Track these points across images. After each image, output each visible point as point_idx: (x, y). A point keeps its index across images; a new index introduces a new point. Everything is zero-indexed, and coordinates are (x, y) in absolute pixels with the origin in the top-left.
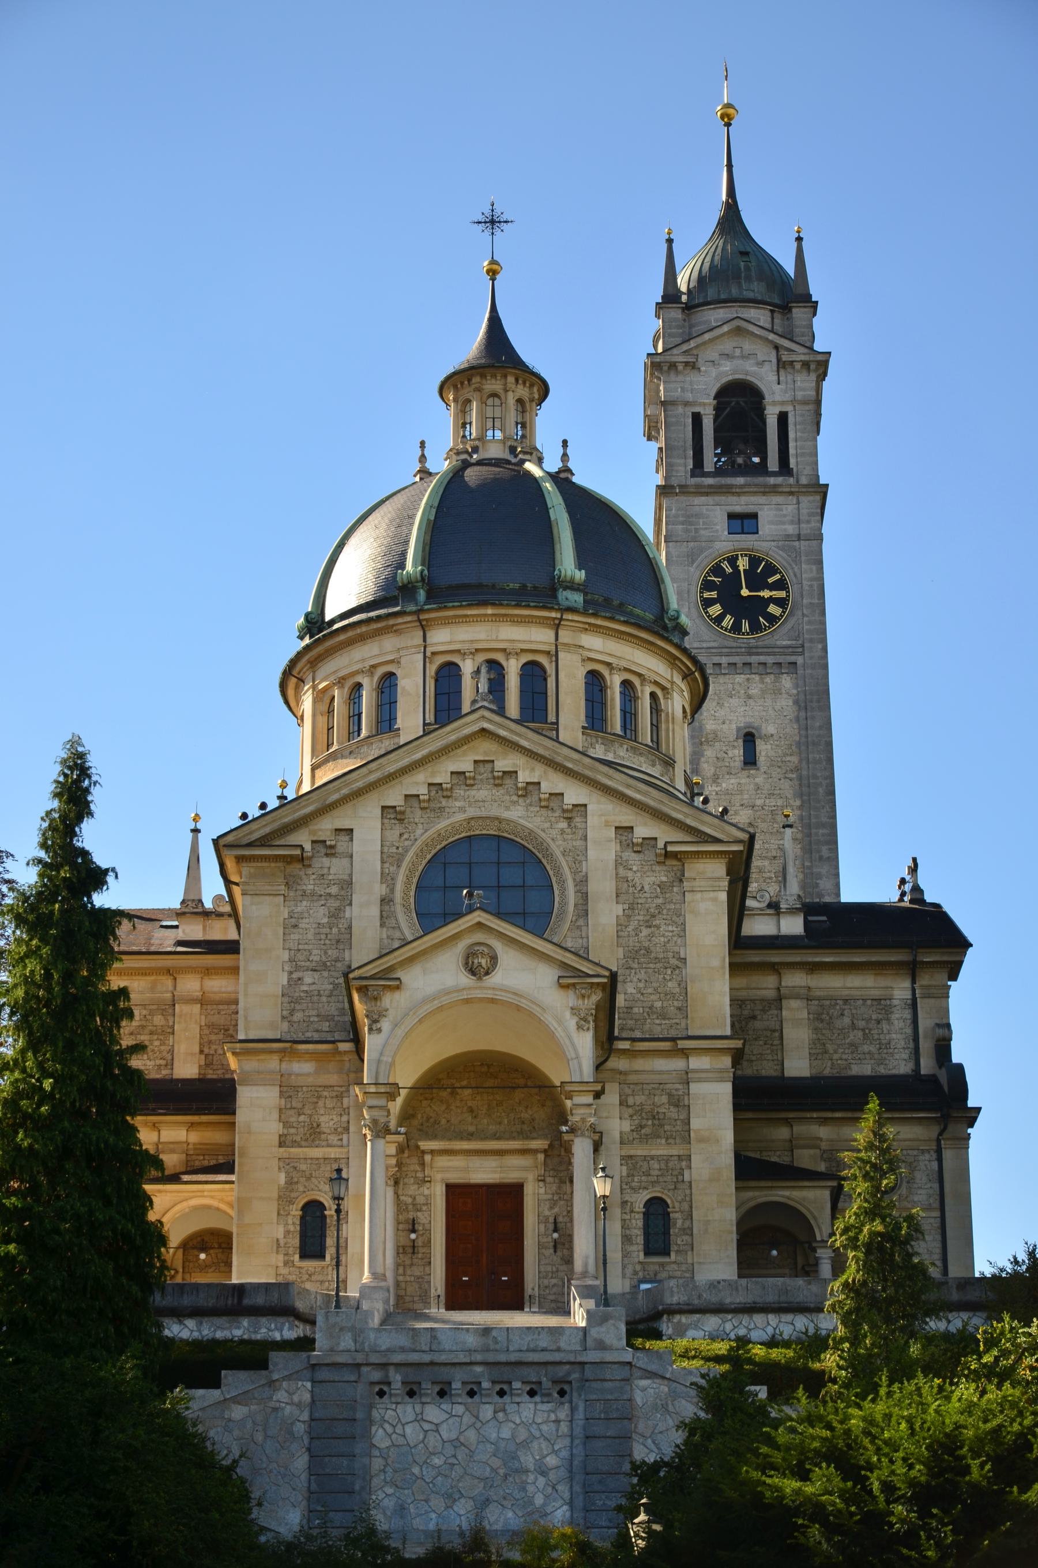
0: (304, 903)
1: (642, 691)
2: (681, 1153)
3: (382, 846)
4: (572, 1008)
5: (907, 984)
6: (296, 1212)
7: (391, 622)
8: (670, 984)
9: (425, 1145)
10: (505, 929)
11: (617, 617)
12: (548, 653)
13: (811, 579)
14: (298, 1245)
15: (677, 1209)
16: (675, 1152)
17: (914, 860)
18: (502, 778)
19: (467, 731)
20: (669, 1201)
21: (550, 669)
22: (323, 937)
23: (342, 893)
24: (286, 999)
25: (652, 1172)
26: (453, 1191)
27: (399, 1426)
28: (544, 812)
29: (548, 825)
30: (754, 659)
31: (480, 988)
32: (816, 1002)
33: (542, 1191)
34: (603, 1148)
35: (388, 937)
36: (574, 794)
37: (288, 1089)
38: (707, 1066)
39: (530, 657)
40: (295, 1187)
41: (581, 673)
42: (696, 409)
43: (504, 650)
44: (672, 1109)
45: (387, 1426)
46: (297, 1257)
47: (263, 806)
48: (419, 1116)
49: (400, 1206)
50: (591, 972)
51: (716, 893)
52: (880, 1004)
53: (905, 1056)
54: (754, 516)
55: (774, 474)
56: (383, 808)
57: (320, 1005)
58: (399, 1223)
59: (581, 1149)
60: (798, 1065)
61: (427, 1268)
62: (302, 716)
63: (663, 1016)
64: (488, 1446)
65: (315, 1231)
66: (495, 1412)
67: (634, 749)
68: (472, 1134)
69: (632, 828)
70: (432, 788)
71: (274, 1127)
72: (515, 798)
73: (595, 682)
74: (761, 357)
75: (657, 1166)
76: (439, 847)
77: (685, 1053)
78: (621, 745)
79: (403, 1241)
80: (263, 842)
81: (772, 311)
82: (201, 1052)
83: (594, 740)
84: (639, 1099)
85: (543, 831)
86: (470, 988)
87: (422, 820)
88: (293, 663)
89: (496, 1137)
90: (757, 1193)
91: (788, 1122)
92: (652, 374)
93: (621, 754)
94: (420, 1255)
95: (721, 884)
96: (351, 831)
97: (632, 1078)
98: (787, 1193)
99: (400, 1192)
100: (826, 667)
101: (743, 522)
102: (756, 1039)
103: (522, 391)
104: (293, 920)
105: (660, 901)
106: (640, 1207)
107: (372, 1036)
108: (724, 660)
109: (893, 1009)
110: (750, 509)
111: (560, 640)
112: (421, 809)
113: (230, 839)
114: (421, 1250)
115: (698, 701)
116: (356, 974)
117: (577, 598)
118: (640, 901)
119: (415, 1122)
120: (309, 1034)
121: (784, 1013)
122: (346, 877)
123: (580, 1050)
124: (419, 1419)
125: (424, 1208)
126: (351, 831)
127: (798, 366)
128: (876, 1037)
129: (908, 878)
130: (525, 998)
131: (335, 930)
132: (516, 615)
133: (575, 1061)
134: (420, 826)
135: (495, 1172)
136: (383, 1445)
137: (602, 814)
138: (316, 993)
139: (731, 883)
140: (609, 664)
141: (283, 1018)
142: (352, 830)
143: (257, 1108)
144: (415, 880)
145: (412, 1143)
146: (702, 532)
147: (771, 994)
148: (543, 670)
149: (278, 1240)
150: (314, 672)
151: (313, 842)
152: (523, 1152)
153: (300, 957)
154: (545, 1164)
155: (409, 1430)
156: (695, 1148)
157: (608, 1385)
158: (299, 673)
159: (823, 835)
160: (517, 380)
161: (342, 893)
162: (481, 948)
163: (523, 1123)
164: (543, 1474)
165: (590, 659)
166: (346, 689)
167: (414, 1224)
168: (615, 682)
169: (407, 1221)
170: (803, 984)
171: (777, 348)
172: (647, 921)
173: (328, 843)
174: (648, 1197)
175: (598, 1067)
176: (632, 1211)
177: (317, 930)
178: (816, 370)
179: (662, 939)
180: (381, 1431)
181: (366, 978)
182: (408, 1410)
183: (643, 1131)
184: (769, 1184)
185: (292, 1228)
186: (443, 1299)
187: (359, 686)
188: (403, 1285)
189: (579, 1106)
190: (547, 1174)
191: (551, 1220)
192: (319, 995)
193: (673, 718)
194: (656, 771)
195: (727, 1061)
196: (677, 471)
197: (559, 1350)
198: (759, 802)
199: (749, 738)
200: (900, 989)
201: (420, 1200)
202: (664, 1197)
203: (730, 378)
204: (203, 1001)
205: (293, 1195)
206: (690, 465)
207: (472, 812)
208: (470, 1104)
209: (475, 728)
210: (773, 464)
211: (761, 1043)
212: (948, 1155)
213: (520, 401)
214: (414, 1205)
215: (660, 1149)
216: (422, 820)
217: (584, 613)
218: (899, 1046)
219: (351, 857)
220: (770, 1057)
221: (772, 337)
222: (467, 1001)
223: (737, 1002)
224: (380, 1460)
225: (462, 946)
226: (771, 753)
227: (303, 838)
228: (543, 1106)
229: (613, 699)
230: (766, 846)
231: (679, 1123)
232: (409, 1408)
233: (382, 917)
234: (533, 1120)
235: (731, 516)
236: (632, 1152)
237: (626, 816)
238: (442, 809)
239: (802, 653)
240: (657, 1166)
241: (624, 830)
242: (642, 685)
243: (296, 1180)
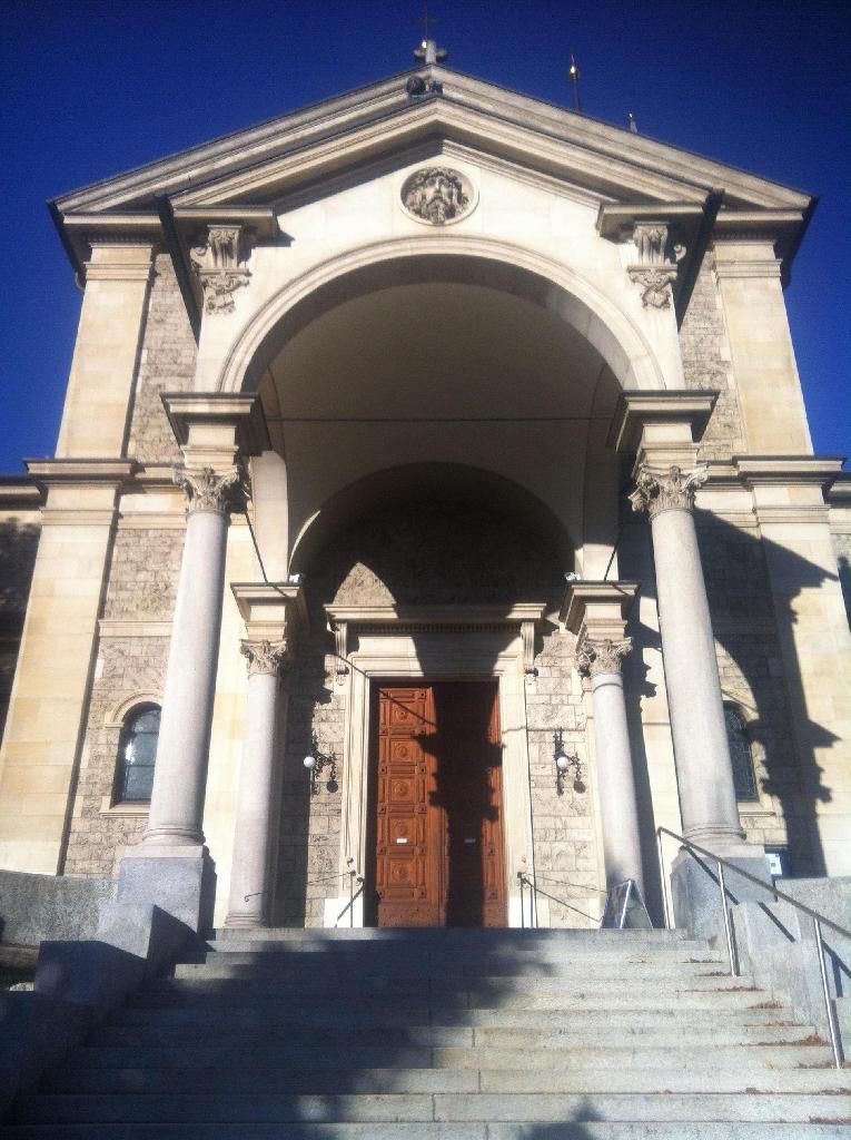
4: (630, 270)
10: (488, 130)
31: (439, 236)
38: (786, 501)
40: (117, 682)
46: (107, 800)
51: (763, 279)
86: (418, 238)
95: (771, 268)
123: (653, 343)
130: (532, 252)
133: (647, 362)
153: (164, 359)
179: (692, 338)
185: (104, 750)
225: (400, 176)
243: (120, 671)
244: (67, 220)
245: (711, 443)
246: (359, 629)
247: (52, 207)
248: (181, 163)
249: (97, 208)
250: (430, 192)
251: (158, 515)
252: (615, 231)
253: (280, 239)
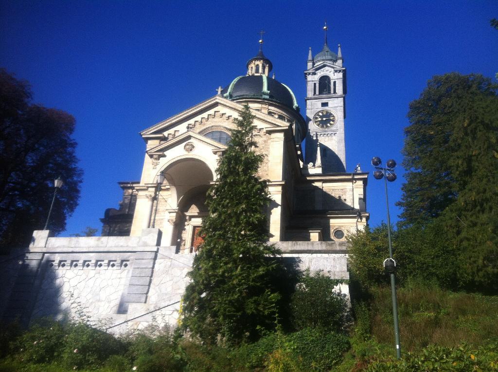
30: (326, 133)
72: (225, 120)
101: (325, 104)
110: (327, 102)
157: (144, 261)
164: (109, 302)
171: (333, 68)
197: (127, 246)
206: (313, 93)
210: (332, 91)
227: (166, 134)
238: (205, 124)
244: (143, 136)
246: (191, 217)
247: (140, 134)
248: (165, 122)
249: (148, 133)
250: (188, 147)
252: (215, 153)
253: (164, 156)
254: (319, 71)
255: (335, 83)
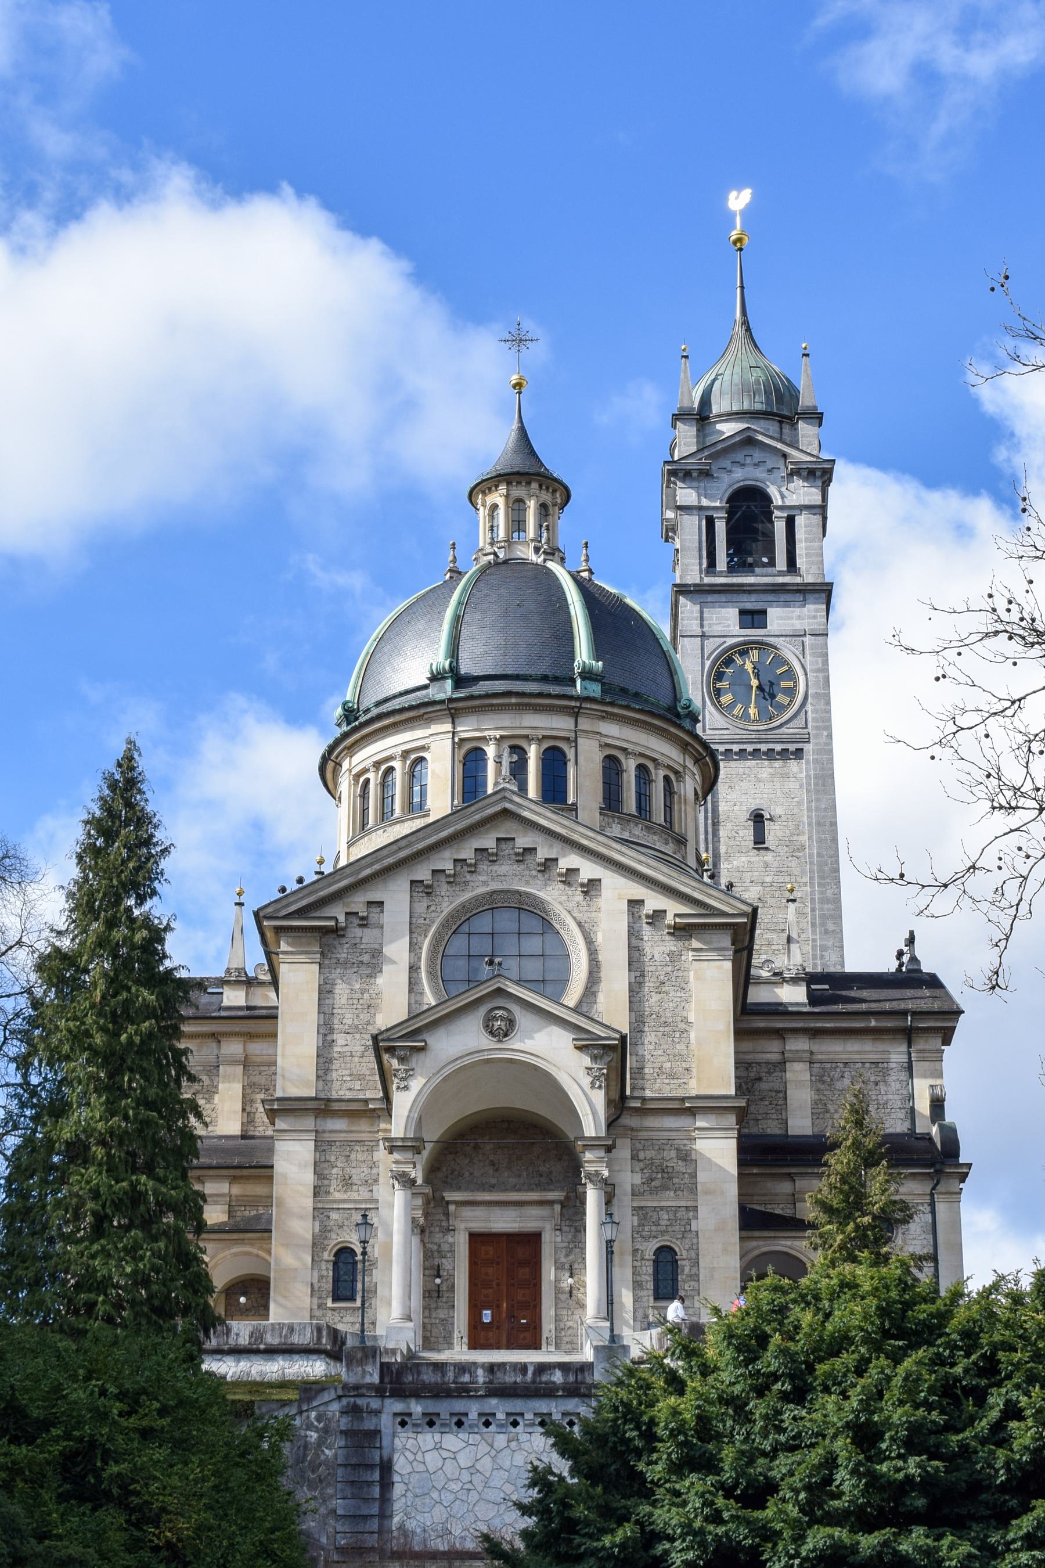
0: (338, 970)
1: (656, 774)
2: (689, 1204)
3: (411, 917)
5: (904, 1048)
6: (328, 1256)
7: (422, 711)
8: (678, 1046)
9: (450, 1196)
11: (633, 705)
12: (567, 739)
13: (818, 671)
14: (331, 1289)
15: (684, 1257)
16: (683, 1204)
17: (912, 933)
18: (523, 854)
19: (490, 811)
20: (677, 1249)
21: (570, 754)
22: (355, 1002)
23: (374, 961)
24: (321, 1060)
25: (662, 1223)
26: (477, 1239)
27: (420, 1453)
28: (561, 886)
29: (564, 898)
32: (818, 1065)
33: (559, 1239)
34: (615, 1201)
35: (416, 1002)
36: (589, 870)
37: (322, 1145)
39: (552, 743)
40: (328, 1234)
41: (598, 757)
42: (709, 513)
43: (526, 737)
44: (680, 1163)
45: (407, 1453)
47: (300, 880)
48: (444, 1169)
49: (428, 1255)
50: (603, 1035)
52: (877, 1067)
53: (902, 1116)
54: (764, 612)
55: (781, 574)
56: (412, 882)
57: (353, 1065)
58: (425, 1269)
59: (592, 1197)
60: (800, 1124)
61: (451, 1312)
62: (340, 798)
63: (672, 1076)
64: (502, 1472)
65: (347, 1274)
66: (509, 1441)
67: (648, 828)
68: (493, 1186)
69: (643, 901)
70: (457, 864)
71: (309, 1177)
72: (534, 873)
73: (612, 767)
74: (770, 465)
75: (666, 1217)
76: (463, 919)
77: (692, 1112)
78: (637, 825)
79: (430, 1286)
80: (300, 913)
81: (781, 422)
82: (244, 1110)
83: (611, 820)
84: (650, 1154)
85: (560, 903)
87: (448, 894)
88: (331, 749)
89: (515, 1188)
90: (761, 1243)
91: (791, 1177)
92: (669, 481)
93: (637, 832)
94: (444, 1300)
96: (381, 904)
97: (644, 1135)
98: (789, 1243)
99: (426, 1240)
100: (830, 752)
102: (761, 1100)
103: (546, 497)
104: (328, 986)
105: (669, 969)
106: (649, 1254)
107: (399, 1093)
108: (736, 748)
109: (891, 1072)
111: (579, 727)
112: (449, 883)
113: (269, 910)
114: (446, 1295)
115: (709, 784)
116: (384, 1036)
117: (595, 689)
118: (650, 969)
119: (440, 1175)
120: (341, 1093)
121: (788, 1075)
122: (377, 946)
124: (438, 1447)
125: (449, 1255)
126: (381, 904)
127: (804, 473)
128: (874, 1097)
129: (905, 949)
131: (366, 996)
132: (539, 705)
134: (446, 899)
135: (515, 1221)
136: (404, 1472)
137: (616, 889)
138: (349, 1054)
139: (736, 952)
140: (624, 750)
141: (318, 1077)
142: (382, 903)
143: (294, 1160)
144: (441, 949)
145: (437, 1195)
146: (715, 628)
147: (775, 1057)
148: (564, 755)
149: (312, 1284)
150: (351, 757)
151: (346, 914)
152: (541, 1203)
154: (562, 1214)
155: (429, 1457)
156: (701, 1199)
158: (337, 758)
159: (829, 910)
160: (540, 486)
161: (374, 961)
162: (500, 1013)
163: (541, 1176)
165: (607, 745)
166: (380, 773)
167: (439, 1271)
168: (630, 765)
169: (432, 1268)
170: (807, 1048)
172: (658, 987)
173: (360, 914)
174: (658, 1245)
175: (610, 1125)
176: (642, 1259)
177: (350, 996)
178: (822, 476)
179: (671, 1004)
180: (402, 1458)
181: (393, 1040)
182: (428, 1439)
183: (653, 1184)
184: (772, 1234)
185: (325, 1273)
186: (465, 1340)
187: (391, 769)
188: (429, 1327)
189: (592, 1162)
190: (563, 1223)
191: (567, 1266)
192: (352, 1056)
193: (685, 800)
194: (669, 849)
195: (731, 1120)
196: (692, 570)
198: (768, 879)
199: (759, 819)
200: (896, 1053)
201: (445, 1247)
202: (673, 1245)
203: (742, 484)
204: (246, 1063)
205: (326, 1242)
207: (494, 886)
208: (491, 1158)
209: (498, 808)
211: (767, 1103)
212: (940, 1207)
213: (543, 507)
214: (439, 1252)
215: (668, 1199)
216: (448, 894)
217: (602, 702)
218: (895, 1106)
219: (382, 927)
220: (774, 1116)
221: (779, 446)
222: (488, 1061)
223: (742, 1064)
224: (402, 1485)
225: (482, 1011)
226: (780, 833)
227: (338, 912)
228: (560, 1160)
229: (629, 782)
230: (775, 920)
231: (686, 1176)
232: (429, 1436)
233: (410, 983)
234: (551, 1173)
235: (742, 613)
236: (643, 1204)
237: (638, 891)
239: (808, 742)
240: (666, 1217)
241: (635, 904)
242: (656, 768)
245: (675, 1081)
251: (341, 1132)
254: (727, 463)
255: (790, 522)
